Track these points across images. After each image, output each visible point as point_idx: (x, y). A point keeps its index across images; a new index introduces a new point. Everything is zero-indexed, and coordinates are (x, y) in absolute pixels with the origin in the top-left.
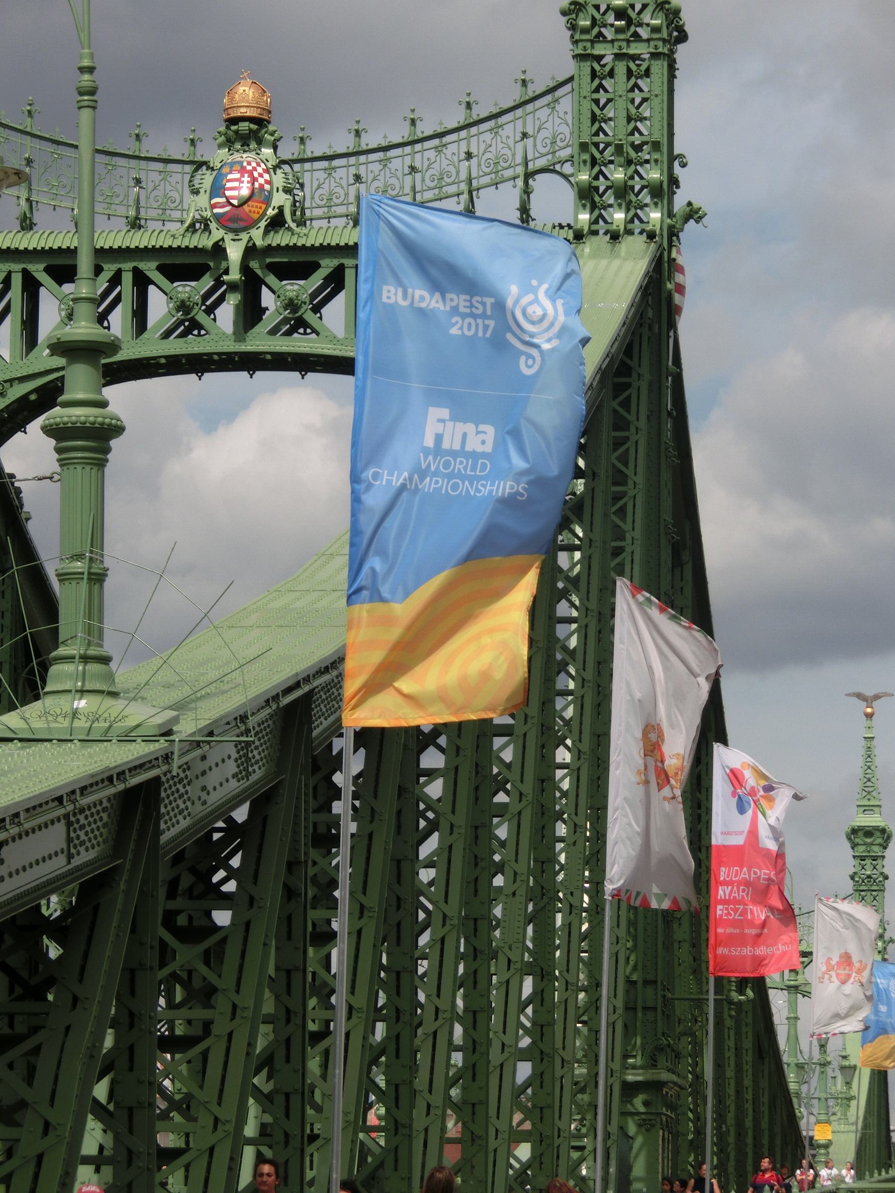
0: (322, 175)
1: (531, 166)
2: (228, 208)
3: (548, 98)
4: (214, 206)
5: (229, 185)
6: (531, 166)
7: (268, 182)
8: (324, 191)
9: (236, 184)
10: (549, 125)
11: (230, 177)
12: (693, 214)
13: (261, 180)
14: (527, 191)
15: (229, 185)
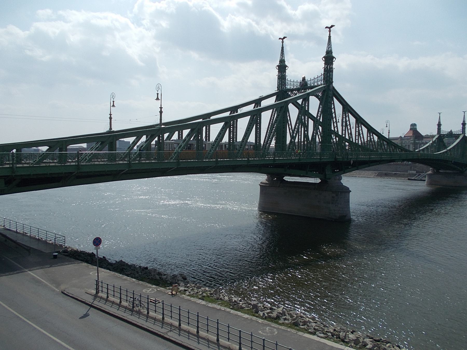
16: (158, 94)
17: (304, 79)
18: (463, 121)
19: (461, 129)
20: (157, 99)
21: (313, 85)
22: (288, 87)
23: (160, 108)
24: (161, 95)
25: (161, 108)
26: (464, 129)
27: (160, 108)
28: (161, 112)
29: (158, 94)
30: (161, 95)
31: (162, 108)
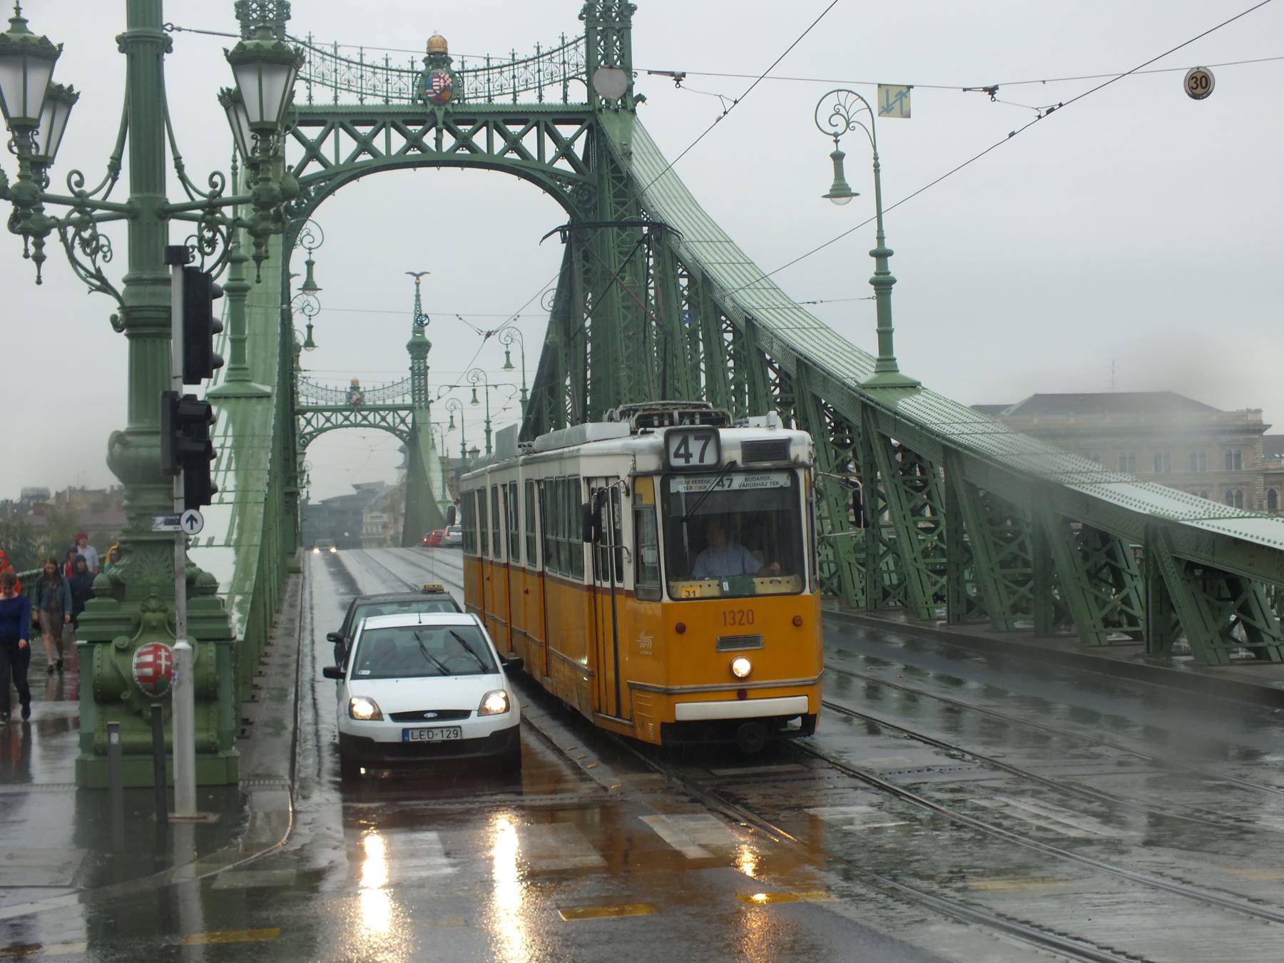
0: (473, 79)
1: (567, 76)
2: (435, 95)
3: (574, 45)
4: (428, 93)
5: (434, 84)
6: (567, 76)
7: (452, 82)
8: (474, 86)
9: (438, 84)
10: (575, 57)
11: (434, 80)
12: (641, 98)
13: (448, 82)
14: (565, 87)
15: (434, 84)
16: (838, 157)
17: (438, 57)
18: (415, 332)
19: (408, 374)
20: (840, 191)
21: (506, 100)
22: (323, 97)
23: (873, 254)
24: (877, 166)
25: (881, 255)
26: (420, 373)
27: (873, 254)
28: (883, 285)
29: (838, 157)
30: (877, 166)
31: (890, 253)
